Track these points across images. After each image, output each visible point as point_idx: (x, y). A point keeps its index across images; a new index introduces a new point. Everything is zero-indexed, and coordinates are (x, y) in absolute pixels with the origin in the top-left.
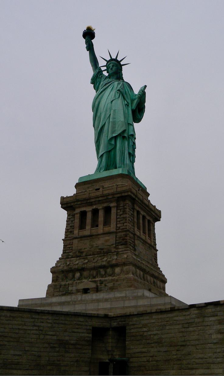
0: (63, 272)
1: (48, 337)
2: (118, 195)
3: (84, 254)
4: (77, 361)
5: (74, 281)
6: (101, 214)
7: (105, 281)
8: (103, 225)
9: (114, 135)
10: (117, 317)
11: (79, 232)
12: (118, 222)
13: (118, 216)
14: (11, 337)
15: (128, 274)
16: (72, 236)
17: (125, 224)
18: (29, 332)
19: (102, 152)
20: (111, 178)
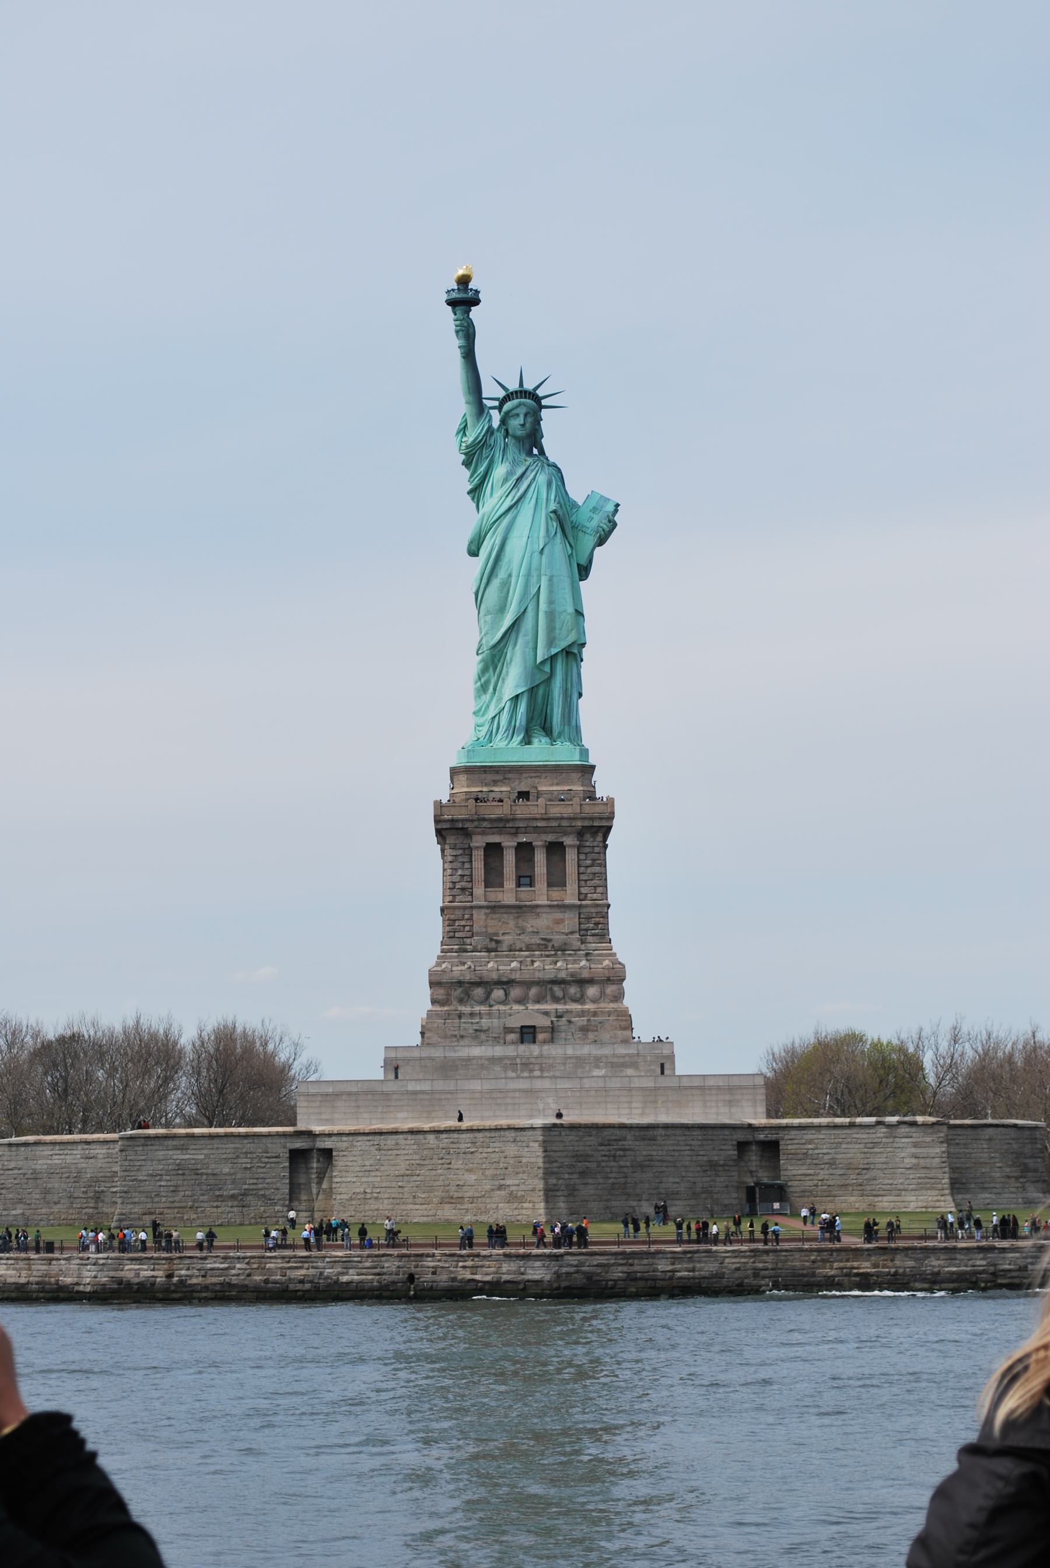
0: (460, 983)
1: (700, 1158)
2: (587, 823)
4: (727, 1186)
5: (491, 1006)
6: (540, 857)
7: (567, 1011)
9: (554, 651)
10: (765, 1127)
12: (583, 883)
13: (582, 869)
14: (669, 1161)
16: (469, 898)
17: (599, 890)
18: (682, 1153)
19: (517, 686)
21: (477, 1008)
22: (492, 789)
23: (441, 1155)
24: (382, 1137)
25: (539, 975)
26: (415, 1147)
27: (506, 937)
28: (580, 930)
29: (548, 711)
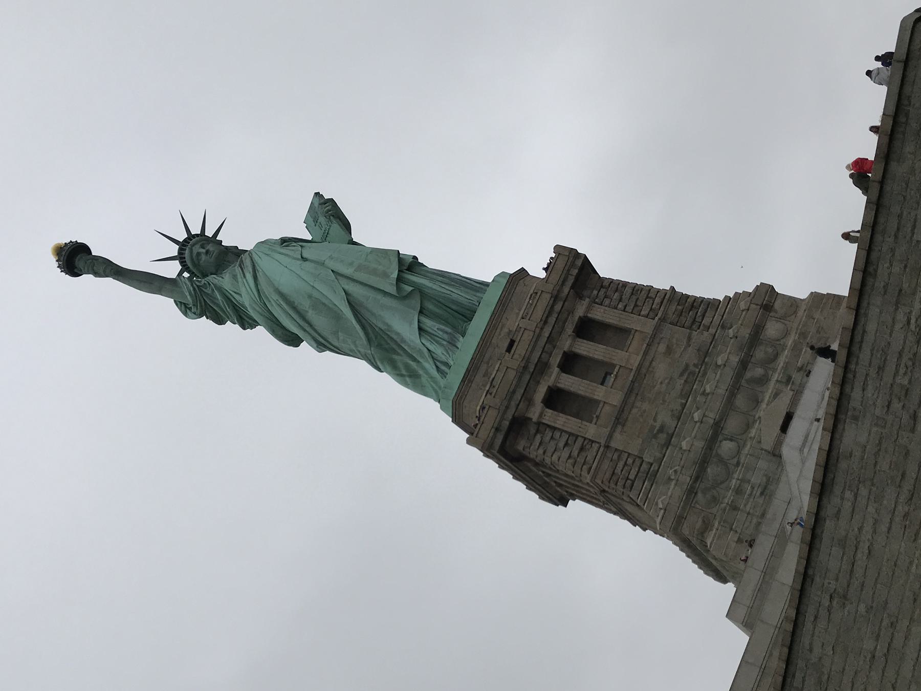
0: (691, 492)
3: (671, 423)
6: (584, 348)
8: (617, 351)
9: (395, 275)
11: (596, 424)
12: (636, 309)
15: (797, 307)
16: (595, 446)
17: (652, 295)
19: (411, 324)
20: (503, 306)
21: (734, 481)
22: (491, 379)
23: (906, 417)
24: (817, 579)
25: (721, 391)
26: (864, 492)
27: (660, 419)
28: (690, 328)
29: (454, 307)
